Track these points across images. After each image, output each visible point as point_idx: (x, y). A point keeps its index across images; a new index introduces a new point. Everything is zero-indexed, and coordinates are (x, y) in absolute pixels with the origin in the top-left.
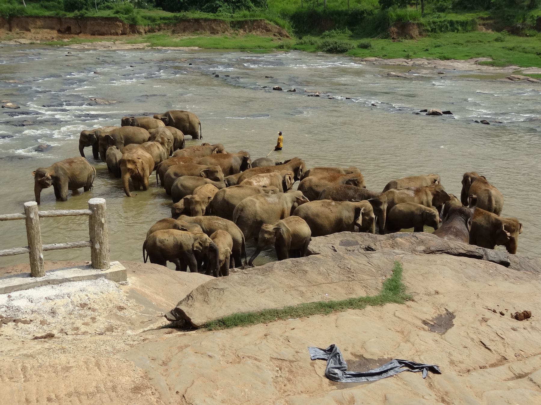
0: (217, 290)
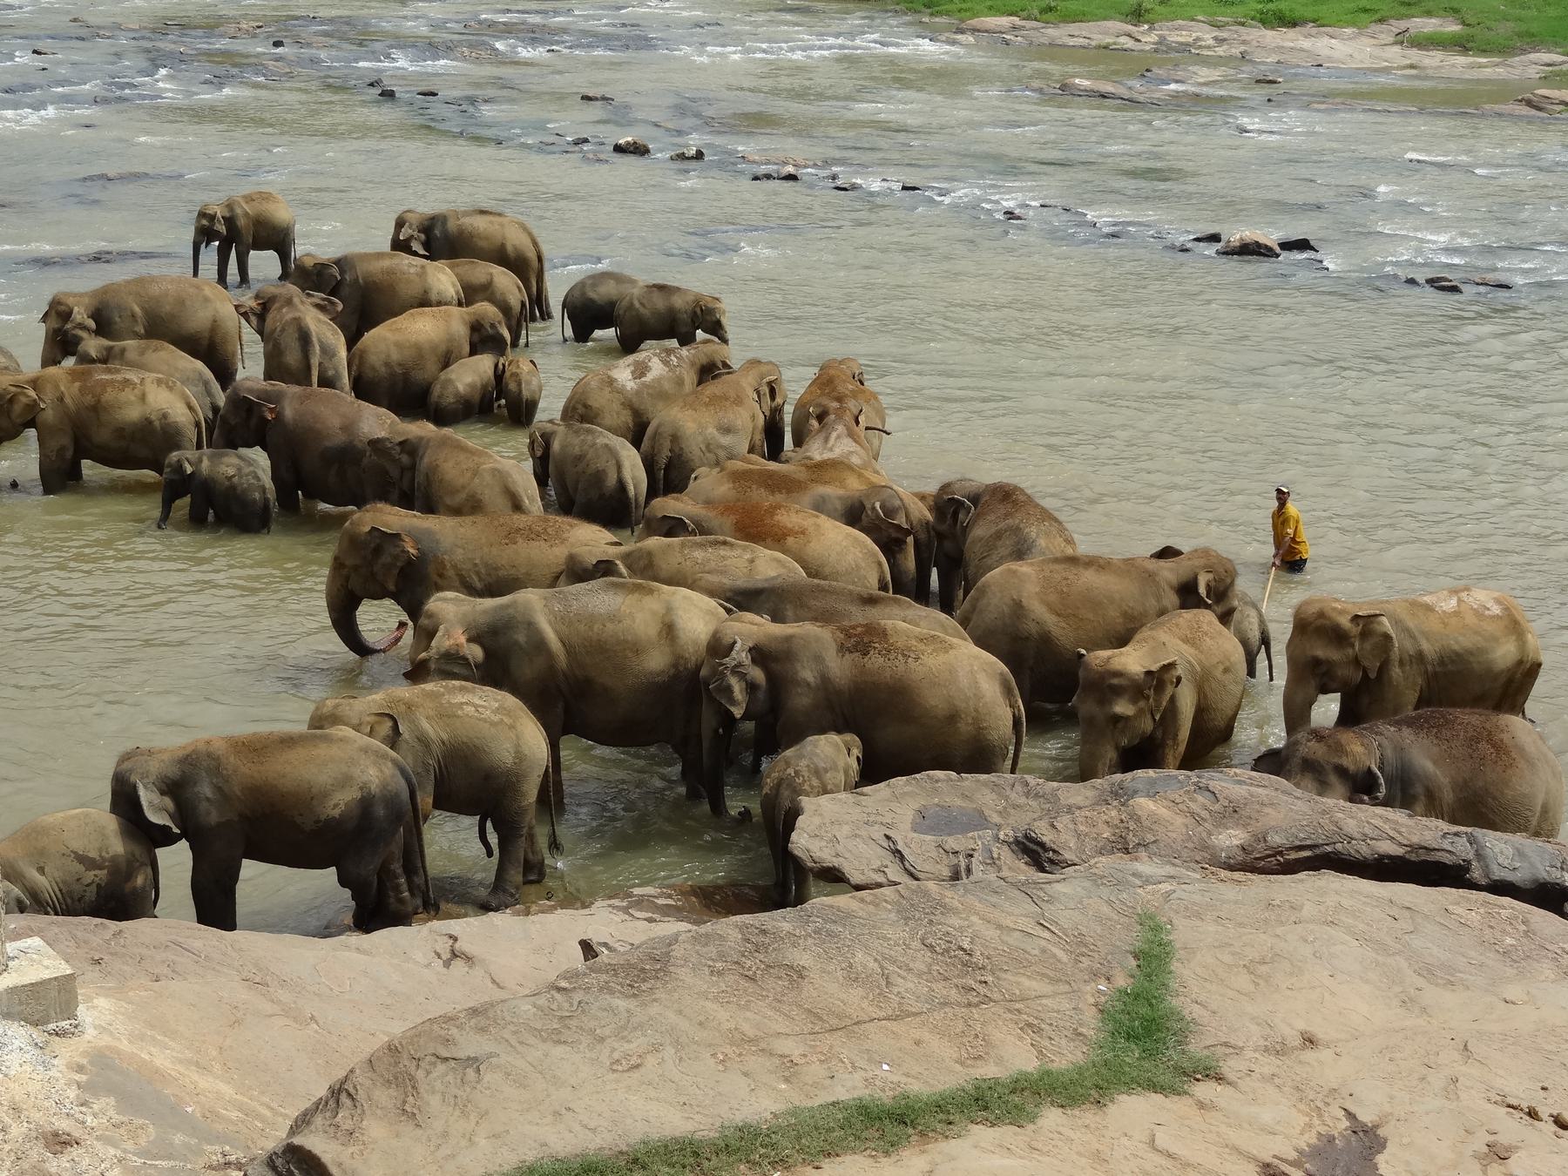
0: (453, 1063)
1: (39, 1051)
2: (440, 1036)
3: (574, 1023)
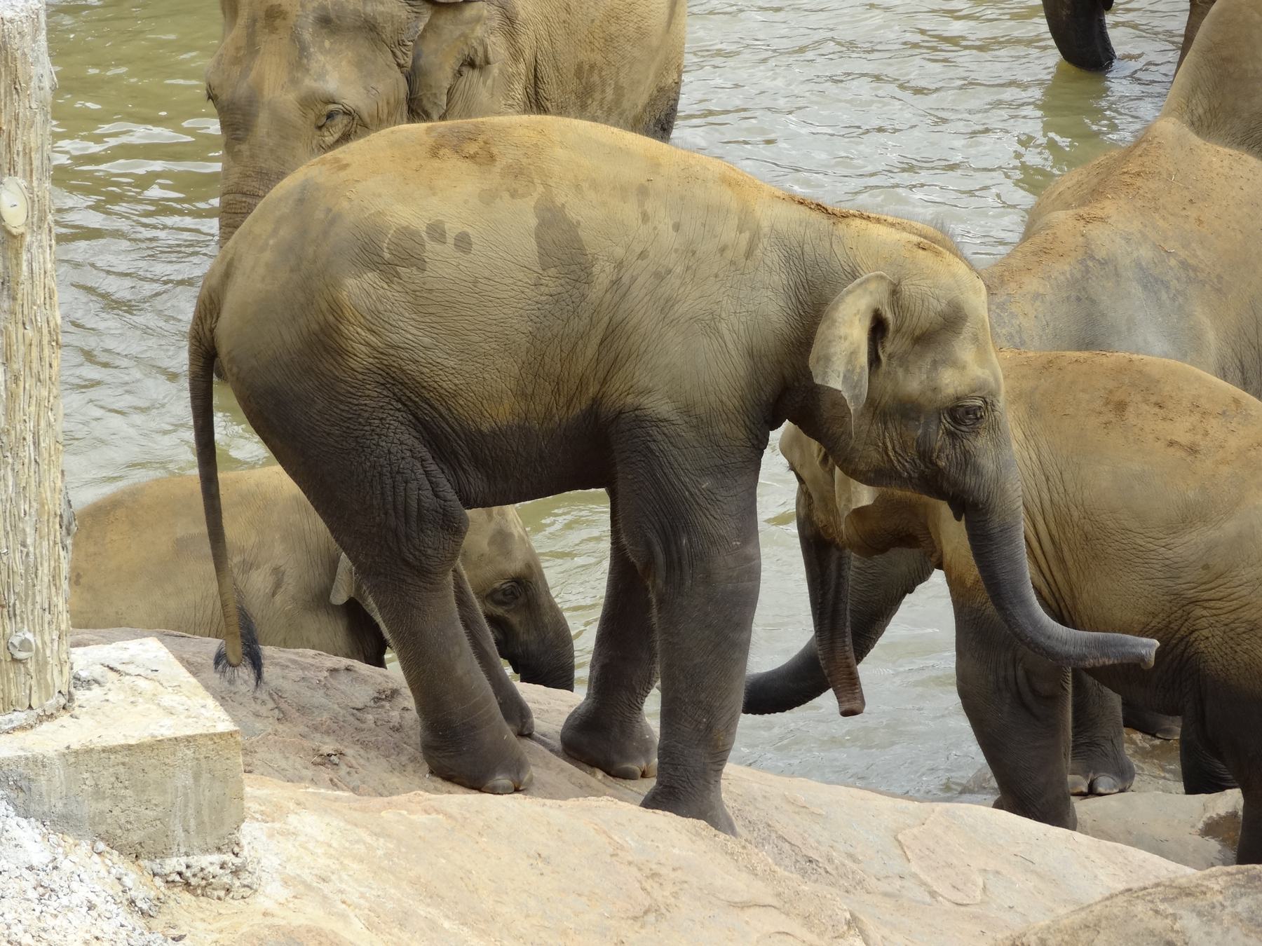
1: (136, 921)
2: (1152, 933)
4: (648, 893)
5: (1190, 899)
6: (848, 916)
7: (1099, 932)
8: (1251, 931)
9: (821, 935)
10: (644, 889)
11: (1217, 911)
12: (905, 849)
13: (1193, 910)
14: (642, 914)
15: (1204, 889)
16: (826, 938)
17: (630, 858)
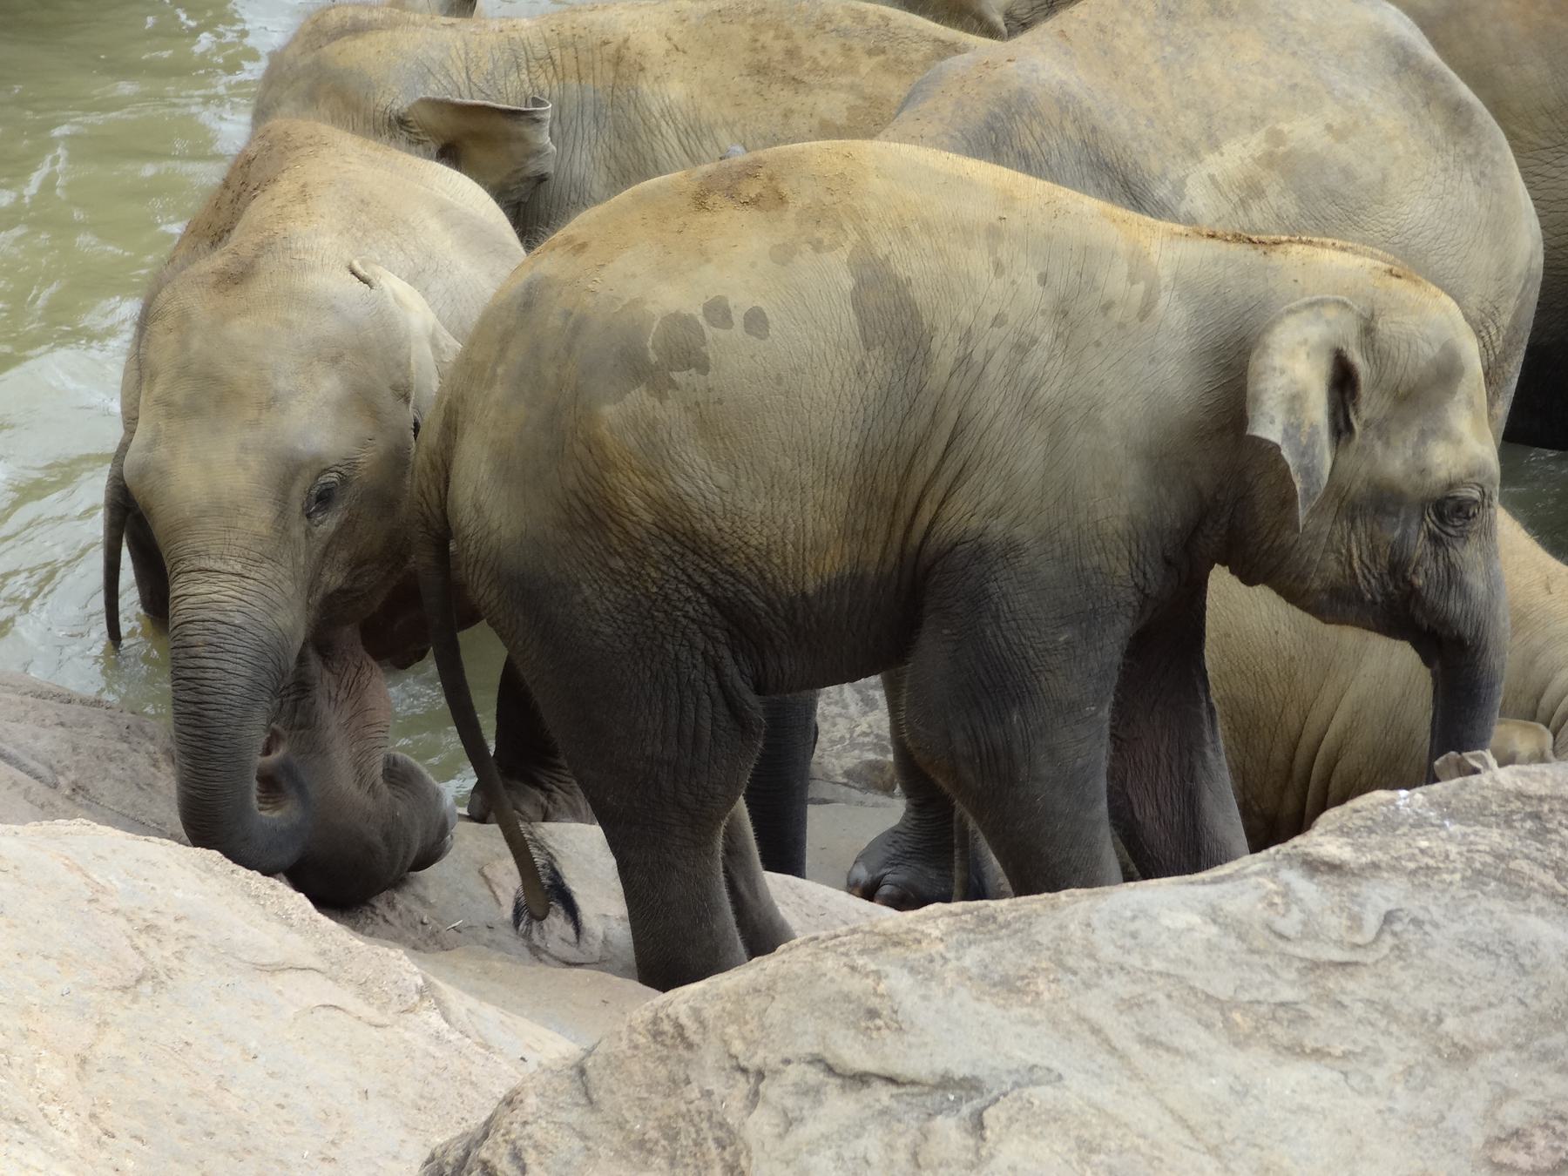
0: (883, 1095)
2: (847, 998)
3: (1359, 987)
4: (142, 954)
5: (899, 950)
6: (420, 982)
7: (773, 998)
8: (983, 993)
9: (383, 1008)
10: (136, 948)
11: (937, 966)
12: (496, 888)
13: (903, 966)
14: (133, 983)
15: (918, 935)
16: (390, 1012)
17: (116, 905)
